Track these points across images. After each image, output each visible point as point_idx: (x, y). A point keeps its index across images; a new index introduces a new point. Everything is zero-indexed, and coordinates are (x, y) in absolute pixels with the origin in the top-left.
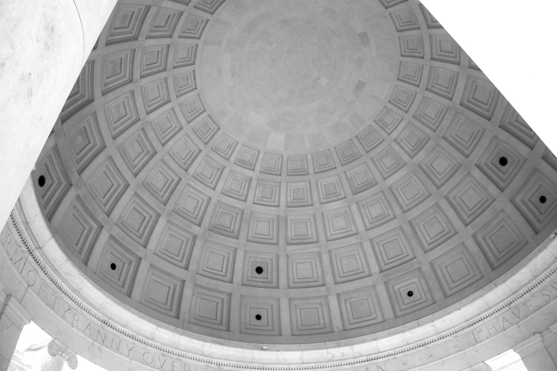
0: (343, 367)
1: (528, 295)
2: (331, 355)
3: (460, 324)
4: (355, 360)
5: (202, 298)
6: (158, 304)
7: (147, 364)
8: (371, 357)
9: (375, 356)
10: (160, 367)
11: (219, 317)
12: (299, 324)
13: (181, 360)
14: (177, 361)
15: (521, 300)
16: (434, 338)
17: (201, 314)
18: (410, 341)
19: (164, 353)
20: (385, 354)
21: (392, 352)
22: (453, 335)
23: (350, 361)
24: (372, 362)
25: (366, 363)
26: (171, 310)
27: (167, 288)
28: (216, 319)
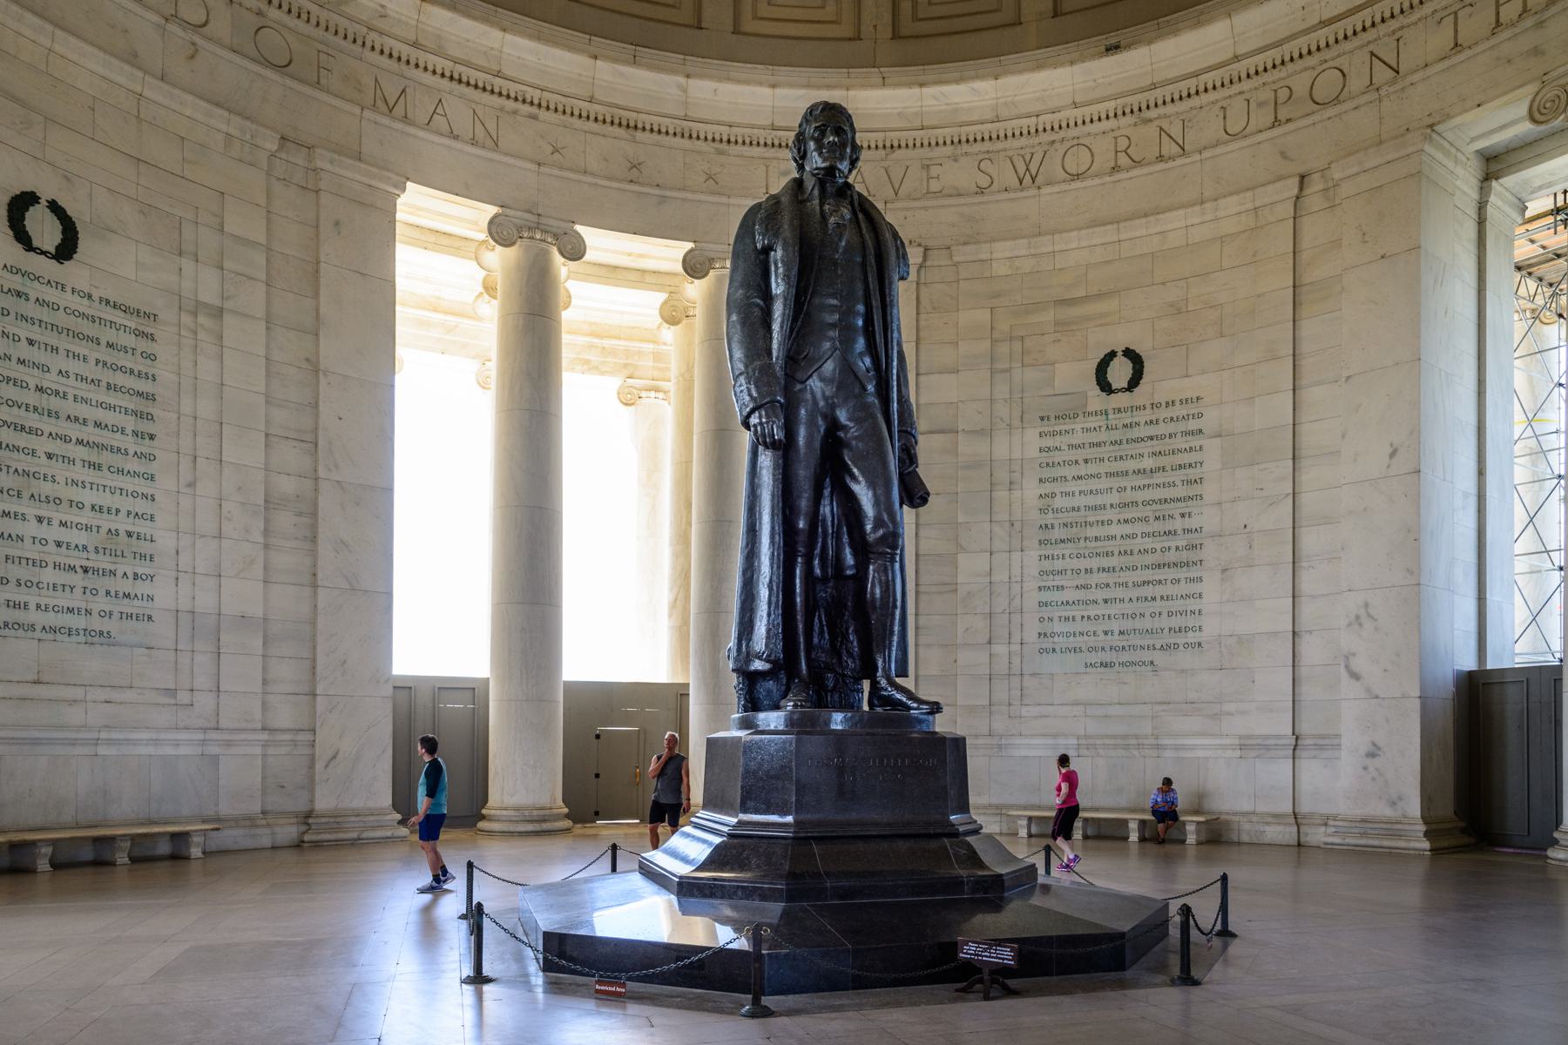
1: (948, 150)
3: (753, 127)
8: (467, 73)
9: (481, 78)
15: (926, 152)
16: (665, 122)
18: (599, 96)
20: (514, 88)
21: (536, 95)
22: (717, 145)
24: (463, 88)
25: (445, 82)
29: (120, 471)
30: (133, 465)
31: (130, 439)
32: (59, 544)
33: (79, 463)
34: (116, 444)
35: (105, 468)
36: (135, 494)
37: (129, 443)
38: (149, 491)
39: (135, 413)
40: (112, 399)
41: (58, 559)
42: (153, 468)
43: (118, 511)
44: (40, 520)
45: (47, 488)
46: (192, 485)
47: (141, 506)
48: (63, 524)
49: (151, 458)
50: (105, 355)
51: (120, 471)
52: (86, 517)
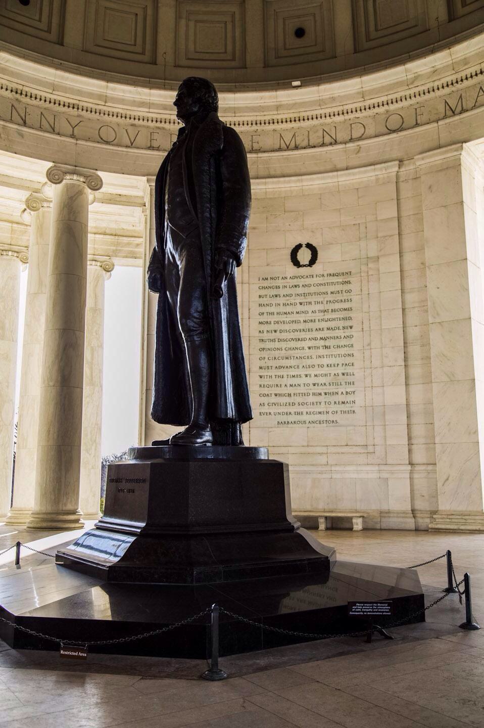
0: (438, 93)
2: (413, 76)
4: (459, 76)
5: (196, 21)
6: (120, 46)
7: (107, 143)
10: (130, 144)
11: (229, 48)
12: (372, 28)
13: (163, 128)
14: (158, 131)
17: (198, 50)
19: (132, 121)
23: (449, 79)
26: (143, 53)
27: (134, 17)
28: (226, 52)
29: (338, 347)
30: (343, 342)
31: (342, 331)
32: (314, 385)
33: (321, 348)
34: (336, 335)
35: (332, 347)
36: (345, 355)
37: (340, 333)
38: (350, 352)
39: (343, 319)
40: (334, 315)
41: (314, 391)
42: (352, 341)
43: (338, 365)
44: (306, 376)
45: (309, 362)
46: (369, 345)
47: (348, 360)
48: (316, 376)
49: (351, 337)
50: (330, 297)
51: (338, 347)
52: (325, 370)
